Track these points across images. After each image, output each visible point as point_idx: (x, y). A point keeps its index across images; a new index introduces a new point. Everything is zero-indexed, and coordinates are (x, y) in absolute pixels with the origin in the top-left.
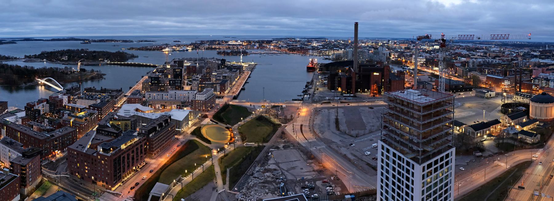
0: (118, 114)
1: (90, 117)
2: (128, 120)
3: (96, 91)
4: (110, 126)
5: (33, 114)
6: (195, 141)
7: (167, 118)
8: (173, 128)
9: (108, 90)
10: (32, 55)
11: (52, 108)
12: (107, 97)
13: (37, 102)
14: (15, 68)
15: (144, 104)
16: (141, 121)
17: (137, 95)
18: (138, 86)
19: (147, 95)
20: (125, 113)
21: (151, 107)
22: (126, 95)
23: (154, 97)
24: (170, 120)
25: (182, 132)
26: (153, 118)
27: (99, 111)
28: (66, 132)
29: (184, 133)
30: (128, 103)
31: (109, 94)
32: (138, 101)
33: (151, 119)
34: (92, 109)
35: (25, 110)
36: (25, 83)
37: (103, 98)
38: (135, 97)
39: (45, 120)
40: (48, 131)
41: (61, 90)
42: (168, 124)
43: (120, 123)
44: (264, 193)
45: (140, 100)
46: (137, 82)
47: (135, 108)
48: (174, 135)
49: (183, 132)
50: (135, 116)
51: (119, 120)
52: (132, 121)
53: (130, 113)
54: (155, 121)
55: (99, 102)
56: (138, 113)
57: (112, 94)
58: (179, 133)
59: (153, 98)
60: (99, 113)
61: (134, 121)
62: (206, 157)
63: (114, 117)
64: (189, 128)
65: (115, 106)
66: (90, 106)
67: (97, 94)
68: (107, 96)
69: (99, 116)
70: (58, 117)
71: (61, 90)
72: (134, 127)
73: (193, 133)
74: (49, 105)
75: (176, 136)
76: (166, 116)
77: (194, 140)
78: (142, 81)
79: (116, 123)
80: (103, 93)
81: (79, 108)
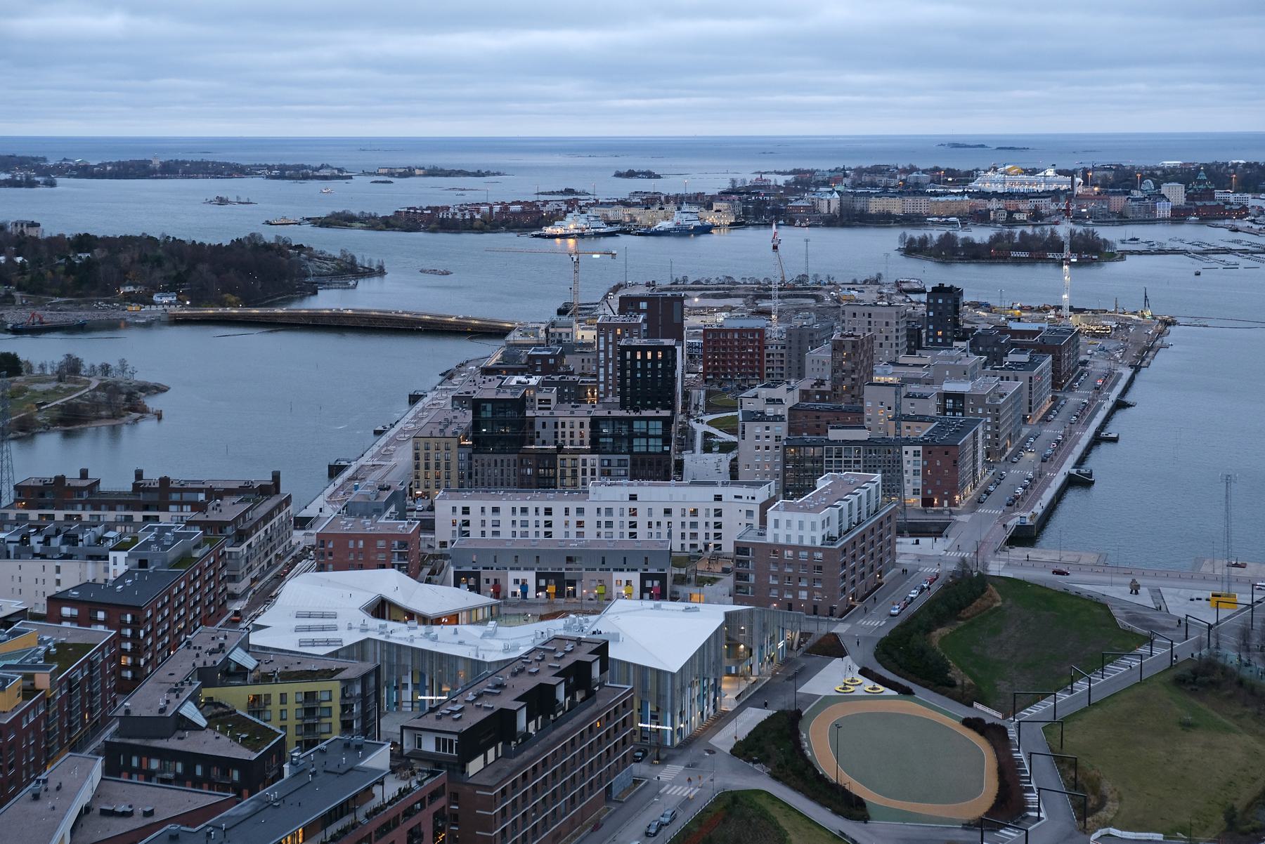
0: (256, 639)
1: (60, 671)
2: (328, 674)
7: (583, 655)
9: (181, 490)
12: (178, 537)
17: (379, 512)
22: (304, 514)
24: (603, 669)
26: (488, 659)
30: (321, 568)
34: (71, 619)
37: (147, 544)
38: (367, 525)
42: (590, 695)
45: (404, 544)
46: (378, 433)
47: (368, 597)
50: (370, 647)
52: (347, 683)
54: (505, 677)
55: (121, 568)
56: (391, 625)
61: (364, 678)
65: (231, 587)
72: (365, 715)
76: (579, 641)
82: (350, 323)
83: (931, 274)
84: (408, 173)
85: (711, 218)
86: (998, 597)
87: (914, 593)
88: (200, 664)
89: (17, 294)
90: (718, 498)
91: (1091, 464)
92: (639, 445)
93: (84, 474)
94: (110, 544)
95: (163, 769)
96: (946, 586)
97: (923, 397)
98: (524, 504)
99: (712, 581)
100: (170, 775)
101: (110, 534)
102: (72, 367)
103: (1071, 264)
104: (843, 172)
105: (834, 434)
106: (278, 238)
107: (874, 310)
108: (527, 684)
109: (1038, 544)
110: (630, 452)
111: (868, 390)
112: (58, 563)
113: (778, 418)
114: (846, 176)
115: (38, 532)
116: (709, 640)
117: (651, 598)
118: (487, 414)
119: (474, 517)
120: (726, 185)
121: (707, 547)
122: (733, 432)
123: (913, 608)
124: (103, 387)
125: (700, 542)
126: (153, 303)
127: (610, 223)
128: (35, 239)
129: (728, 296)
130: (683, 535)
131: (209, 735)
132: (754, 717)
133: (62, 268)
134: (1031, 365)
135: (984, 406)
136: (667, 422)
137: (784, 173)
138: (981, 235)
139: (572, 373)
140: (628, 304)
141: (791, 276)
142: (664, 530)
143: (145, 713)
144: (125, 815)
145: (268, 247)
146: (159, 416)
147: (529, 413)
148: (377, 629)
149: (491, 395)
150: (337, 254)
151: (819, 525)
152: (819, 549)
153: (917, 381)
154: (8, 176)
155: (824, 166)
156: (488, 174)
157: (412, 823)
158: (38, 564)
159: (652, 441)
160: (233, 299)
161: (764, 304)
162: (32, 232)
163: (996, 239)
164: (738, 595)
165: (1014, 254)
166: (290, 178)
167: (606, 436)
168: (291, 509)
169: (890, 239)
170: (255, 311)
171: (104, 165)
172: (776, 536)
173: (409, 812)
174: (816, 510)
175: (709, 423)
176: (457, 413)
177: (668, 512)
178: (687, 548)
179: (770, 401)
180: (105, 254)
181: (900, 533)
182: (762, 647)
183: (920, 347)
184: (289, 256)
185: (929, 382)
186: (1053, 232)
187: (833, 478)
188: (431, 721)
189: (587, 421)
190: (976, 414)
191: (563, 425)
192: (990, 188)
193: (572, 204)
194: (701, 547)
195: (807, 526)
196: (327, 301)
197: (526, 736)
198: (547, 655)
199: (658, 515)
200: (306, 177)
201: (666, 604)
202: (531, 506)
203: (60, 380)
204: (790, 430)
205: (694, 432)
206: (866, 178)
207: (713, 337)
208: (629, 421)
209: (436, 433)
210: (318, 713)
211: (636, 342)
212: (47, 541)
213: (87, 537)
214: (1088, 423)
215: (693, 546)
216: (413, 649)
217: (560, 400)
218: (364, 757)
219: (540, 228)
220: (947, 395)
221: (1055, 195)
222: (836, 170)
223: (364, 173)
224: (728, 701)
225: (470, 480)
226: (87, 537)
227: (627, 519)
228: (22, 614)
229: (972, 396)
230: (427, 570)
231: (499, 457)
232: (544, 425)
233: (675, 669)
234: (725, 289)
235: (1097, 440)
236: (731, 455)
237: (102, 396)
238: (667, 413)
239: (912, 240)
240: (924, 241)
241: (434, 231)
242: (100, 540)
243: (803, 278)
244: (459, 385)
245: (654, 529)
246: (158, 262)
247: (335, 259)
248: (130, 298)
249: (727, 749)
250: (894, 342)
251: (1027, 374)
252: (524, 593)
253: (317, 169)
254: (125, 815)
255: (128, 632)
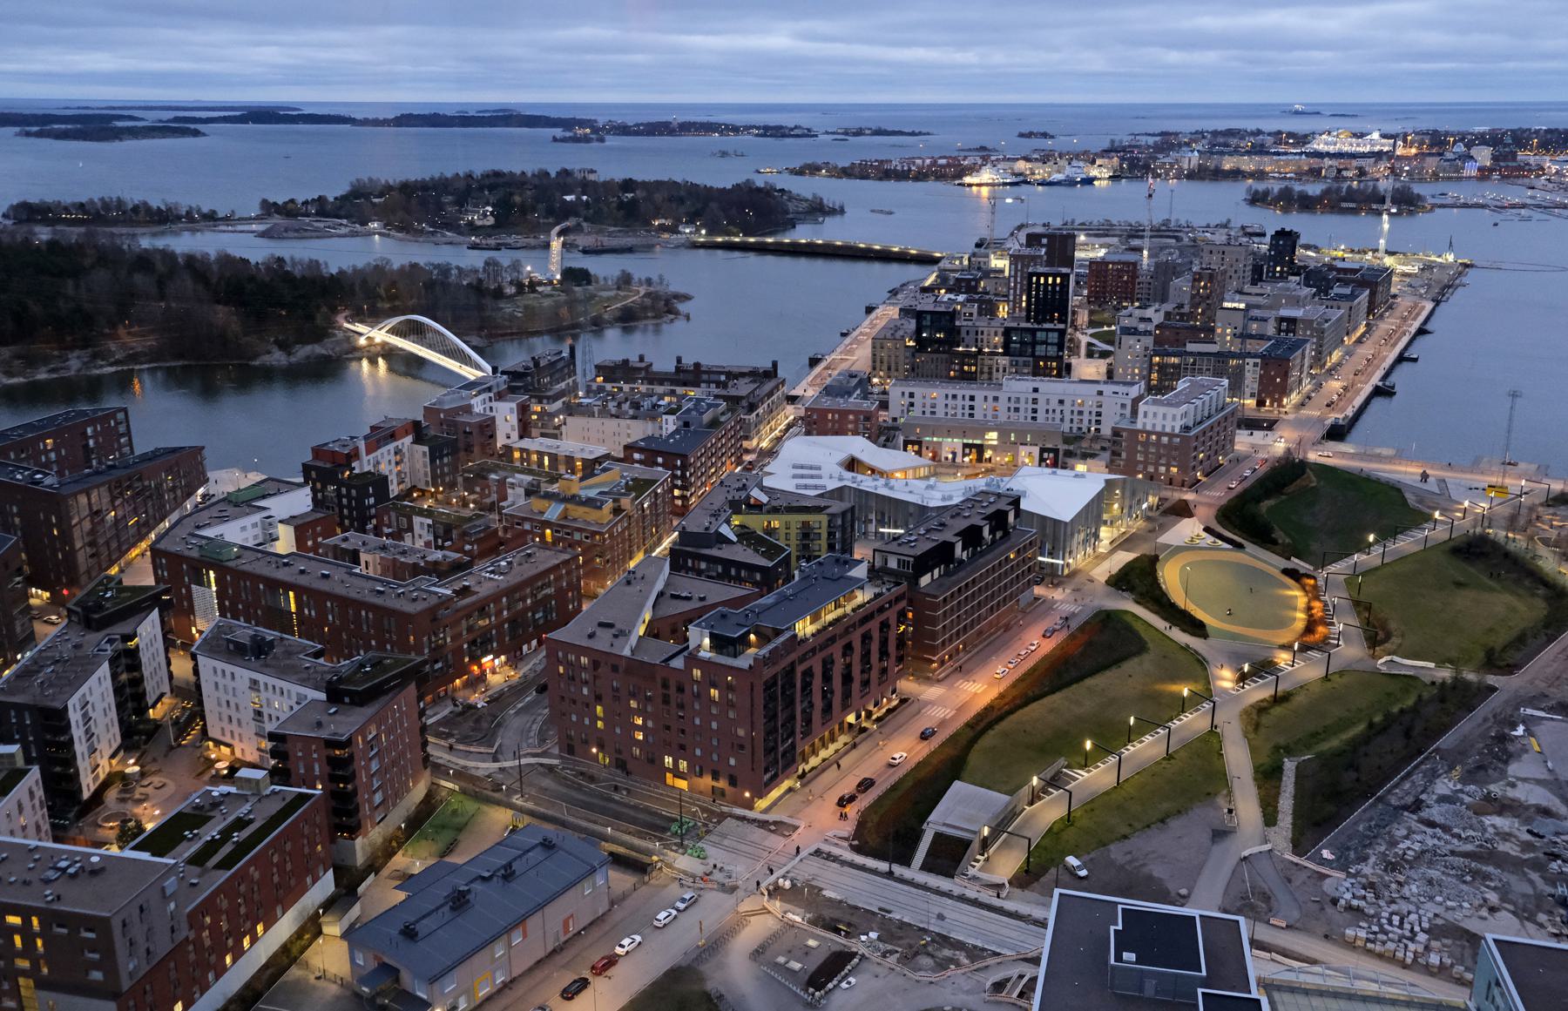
3: (661, 379)
4: (735, 539)
5: (348, 496)
6: (1128, 618)
8: (1029, 554)
9: (709, 372)
10: (300, 199)
11: (442, 465)
12: (710, 406)
13: (366, 438)
14: (215, 268)
15: (884, 436)
16: (873, 517)
18: (851, 352)
19: (897, 393)
20: (795, 476)
21: (919, 453)
23: (933, 406)
25: (1066, 571)
26: (931, 505)
27: (675, 467)
28: (529, 571)
29: (1078, 579)
30: (808, 433)
31: (714, 389)
32: (856, 422)
33: (923, 509)
34: (640, 462)
35: (306, 483)
36: (284, 346)
37: (689, 410)
38: (841, 403)
39: (417, 520)
40: (440, 571)
41: (480, 374)
42: (1006, 534)
43: (776, 524)
44: (1477, 903)
45: (867, 419)
46: (844, 335)
47: (842, 456)
48: (1029, 584)
49: (1074, 574)
50: (847, 491)
51: (775, 510)
53: (820, 477)
55: (672, 428)
56: (860, 477)
57: (733, 392)
58: (1052, 576)
59: (928, 410)
60: (674, 477)
62: (1186, 692)
63: (749, 497)
64: (1101, 558)
65: (746, 444)
66: (629, 448)
67: (660, 389)
68: (710, 400)
69: (677, 492)
70: (474, 502)
71: (480, 374)
73: (1121, 581)
74: (426, 449)
75: (1038, 590)
77: (1126, 612)
78: (869, 327)
79: (757, 522)
80: (685, 384)
81: (578, 455)
82: (820, 250)
83: (1272, 221)
84: (859, 133)
85: (1094, 172)
86: (1314, 479)
87: (1248, 473)
88: (730, 498)
89: (585, 224)
90: (1100, 393)
91: (1392, 379)
92: (1040, 350)
93: (641, 359)
94: (662, 409)
95: (708, 569)
96: (1273, 469)
97: (1265, 320)
98: (954, 392)
99: (1093, 456)
100: (714, 574)
101: (661, 403)
102: (625, 280)
103: (1390, 214)
104: (1200, 134)
105: (1191, 347)
106: (766, 183)
107: (1226, 249)
108: (962, 524)
109: (1349, 438)
110: (1033, 355)
111: (1219, 313)
112: (629, 422)
113: (1147, 333)
114: (1204, 137)
115: (613, 399)
116: (1093, 500)
117: (1047, 466)
118: (927, 322)
119: (917, 400)
120: (1106, 145)
121: (1089, 430)
122: (1111, 343)
123: (1246, 484)
124: (648, 295)
125: (1084, 427)
126: (679, 232)
127: (1014, 174)
128: (594, 182)
129: (1107, 236)
130: (1072, 421)
131: (739, 548)
132: (1124, 557)
133: (614, 205)
134: (1352, 297)
135: (1312, 330)
136: (1062, 333)
137: (1154, 135)
138: (1314, 189)
139: (988, 293)
140: (1033, 240)
141: (1157, 220)
142: (1058, 416)
143: (695, 530)
144: (688, 599)
145: (759, 190)
146: (688, 317)
147: (957, 323)
148: (849, 479)
149: (930, 308)
150: (810, 197)
151: (1179, 417)
152: (1177, 436)
153: (1258, 307)
154: (571, 134)
155: (1186, 127)
156: (920, 134)
157: (883, 617)
158: (615, 421)
159: (1049, 348)
160: (735, 230)
161: (1135, 242)
162: (592, 177)
163: (1326, 192)
164: (1111, 467)
165: (1344, 205)
166: (771, 136)
167: (1015, 342)
168: (784, 389)
169: (1240, 189)
170: (752, 240)
171: (637, 125)
172: (1145, 424)
173: (881, 610)
174: (1178, 405)
175: (1091, 335)
176: (903, 321)
177: (1061, 402)
178: (1075, 430)
179: (1142, 320)
180: (644, 194)
181: (1239, 427)
182: (1131, 507)
183: (1261, 280)
184: (775, 197)
185: (1270, 308)
186: (1375, 187)
187: (1190, 381)
188: (893, 547)
189: (1001, 330)
190: (1305, 335)
191: (982, 333)
192: (1322, 147)
193: (985, 159)
194: (1085, 430)
195: (1169, 417)
196: (802, 234)
197: (961, 562)
198: (977, 505)
199: (1054, 404)
200: (784, 136)
201: (1059, 471)
202: (960, 393)
203: (619, 289)
204: (1156, 343)
205: (1080, 342)
206: (1221, 140)
207: (1097, 267)
208: (1033, 332)
209: (889, 336)
210: (812, 536)
211: (1041, 269)
212: (619, 405)
213: (646, 404)
214: (1394, 345)
215: (1080, 429)
216: (877, 495)
217: (980, 314)
218: (850, 569)
219: (961, 178)
220: (1282, 319)
221: (1378, 156)
222: (1196, 132)
223: (827, 133)
224: (1104, 546)
225: (915, 373)
226: (646, 404)
227: (1030, 406)
228: (607, 457)
229: (1303, 321)
230: (883, 438)
231: (935, 356)
232: (968, 333)
233: (1068, 520)
234: (1102, 231)
235: (1401, 359)
236: (1108, 361)
237: (648, 301)
238: (1062, 326)
239: (1257, 192)
240: (1266, 193)
241: (881, 179)
242: (655, 406)
243: (1166, 222)
244: (904, 299)
245: (1051, 415)
246: (681, 201)
247: (807, 200)
248: (662, 228)
249: (1103, 579)
250: (1241, 275)
251: (1348, 304)
252: (954, 459)
253: (792, 129)
254: (688, 599)
255: (679, 473)
